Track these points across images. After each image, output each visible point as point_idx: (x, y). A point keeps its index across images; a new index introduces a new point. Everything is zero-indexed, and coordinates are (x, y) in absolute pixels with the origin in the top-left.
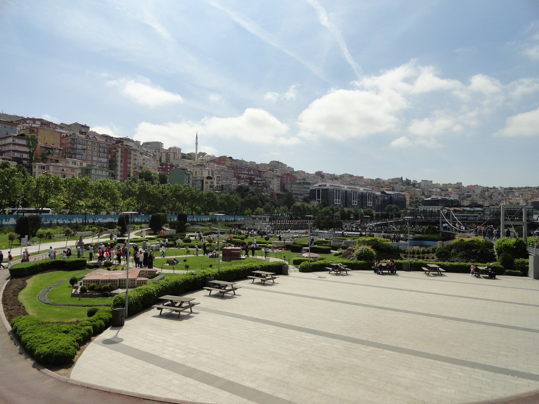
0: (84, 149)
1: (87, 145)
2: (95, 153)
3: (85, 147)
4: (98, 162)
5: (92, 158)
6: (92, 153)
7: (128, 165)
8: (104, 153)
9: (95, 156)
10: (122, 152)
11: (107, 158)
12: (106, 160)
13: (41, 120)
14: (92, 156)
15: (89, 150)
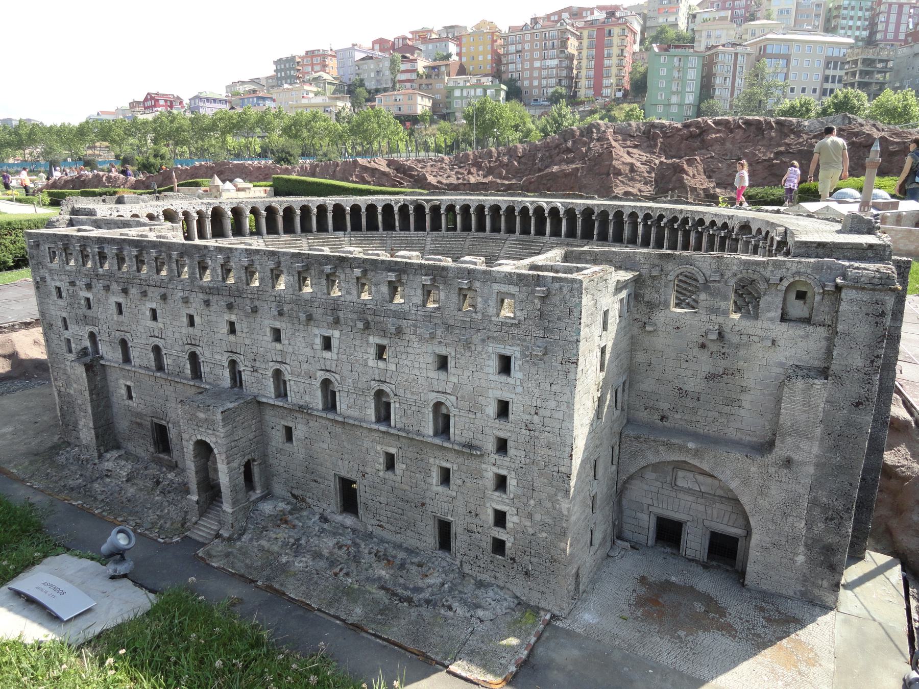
0: (520, 51)
1: (523, 42)
2: (536, 55)
3: (520, 47)
4: (541, 69)
5: (532, 64)
6: (532, 54)
7: (606, 62)
8: (553, 48)
9: (537, 60)
10: (590, 37)
11: (558, 58)
12: (554, 63)
13: (568, 9)
14: (532, 60)
15: (527, 51)
